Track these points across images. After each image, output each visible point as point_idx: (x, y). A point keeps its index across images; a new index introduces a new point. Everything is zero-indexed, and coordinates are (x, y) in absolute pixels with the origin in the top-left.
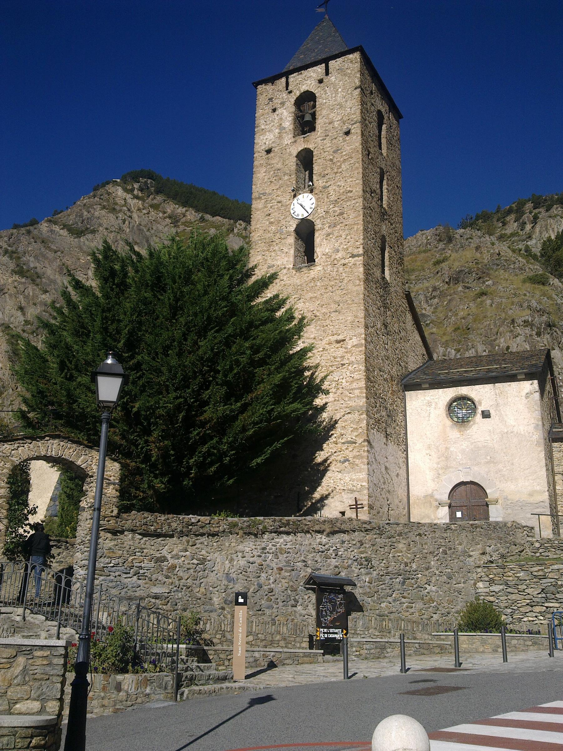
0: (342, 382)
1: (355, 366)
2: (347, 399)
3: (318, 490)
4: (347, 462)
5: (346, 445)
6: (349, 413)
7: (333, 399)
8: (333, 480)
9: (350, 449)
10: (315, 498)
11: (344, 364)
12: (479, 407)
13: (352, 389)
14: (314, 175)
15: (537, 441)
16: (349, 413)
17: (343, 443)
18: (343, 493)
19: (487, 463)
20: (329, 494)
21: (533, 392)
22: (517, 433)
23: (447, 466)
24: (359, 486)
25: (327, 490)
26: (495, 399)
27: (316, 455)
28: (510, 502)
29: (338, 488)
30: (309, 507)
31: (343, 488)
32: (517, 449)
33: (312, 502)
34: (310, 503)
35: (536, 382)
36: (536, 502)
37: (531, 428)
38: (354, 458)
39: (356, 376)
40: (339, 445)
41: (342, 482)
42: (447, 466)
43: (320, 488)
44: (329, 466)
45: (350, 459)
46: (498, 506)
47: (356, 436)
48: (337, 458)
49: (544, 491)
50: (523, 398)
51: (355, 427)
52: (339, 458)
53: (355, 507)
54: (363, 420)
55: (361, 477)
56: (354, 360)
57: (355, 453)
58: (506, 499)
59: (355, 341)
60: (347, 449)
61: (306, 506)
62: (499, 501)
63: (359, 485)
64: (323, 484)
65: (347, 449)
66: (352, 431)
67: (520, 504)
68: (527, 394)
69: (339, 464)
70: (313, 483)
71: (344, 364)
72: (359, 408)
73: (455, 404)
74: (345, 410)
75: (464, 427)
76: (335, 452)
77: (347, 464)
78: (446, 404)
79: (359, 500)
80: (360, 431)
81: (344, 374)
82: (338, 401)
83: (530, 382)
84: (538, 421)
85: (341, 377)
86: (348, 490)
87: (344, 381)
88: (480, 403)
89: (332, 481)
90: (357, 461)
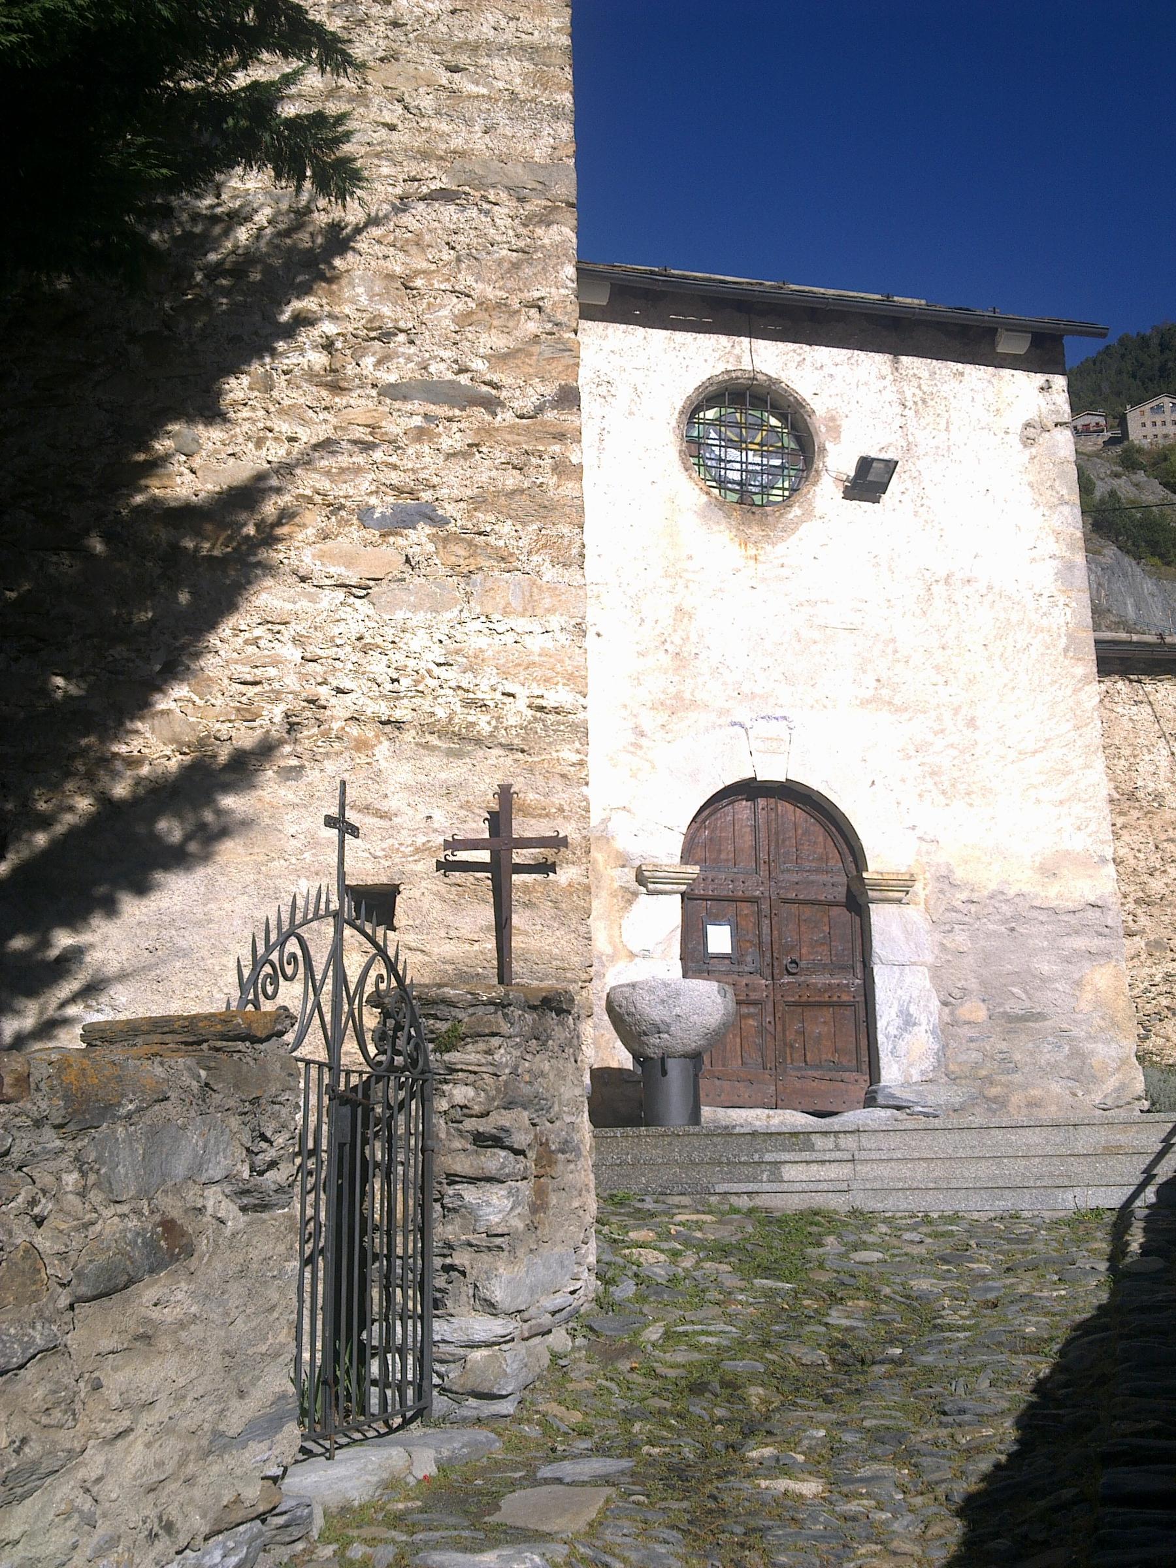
2: (427, 103)
3: (163, 703)
4: (423, 531)
5: (415, 406)
6: (444, 196)
8: (297, 641)
9: (451, 440)
10: (133, 762)
12: (829, 446)
15: (1069, 636)
18: (383, 749)
19: (864, 703)
20: (266, 750)
21: (1050, 425)
22: (990, 588)
23: (678, 696)
24: (517, 712)
25: (248, 714)
26: (899, 421)
27: (162, 445)
28: (964, 896)
29: (339, 708)
30: (73, 833)
32: (989, 659)
33: (105, 800)
34: (84, 804)
35: (1060, 382)
36: (1071, 906)
37: (1045, 576)
38: (478, 502)
42: (678, 696)
43: (180, 691)
44: (268, 537)
45: (449, 509)
46: (914, 913)
47: (499, 358)
48: (338, 491)
49: (1103, 860)
50: (1015, 440)
51: (492, 293)
52: (359, 489)
53: (484, 856)
54: (554, 255)
55: (535, 644)
58: (946, 880)
61: (45, 822)
62: (918, 886)
63: (521, 703)
64: (210, 664)
66: (464, 320)
67: (1005, 908)
68: (1028, 425)
69: (356, 533)
70: (119, 651)
73: (711, 414)
75: (762, 523)
77: (419, 537)
78: (679, 405)
79: (527, 812)
80: (532, 327)
83: (1039, 379)
84: (1071, 546)
86: (430, 727)
88: (835, 430)
89: (294, 654)
90: (506, 528)
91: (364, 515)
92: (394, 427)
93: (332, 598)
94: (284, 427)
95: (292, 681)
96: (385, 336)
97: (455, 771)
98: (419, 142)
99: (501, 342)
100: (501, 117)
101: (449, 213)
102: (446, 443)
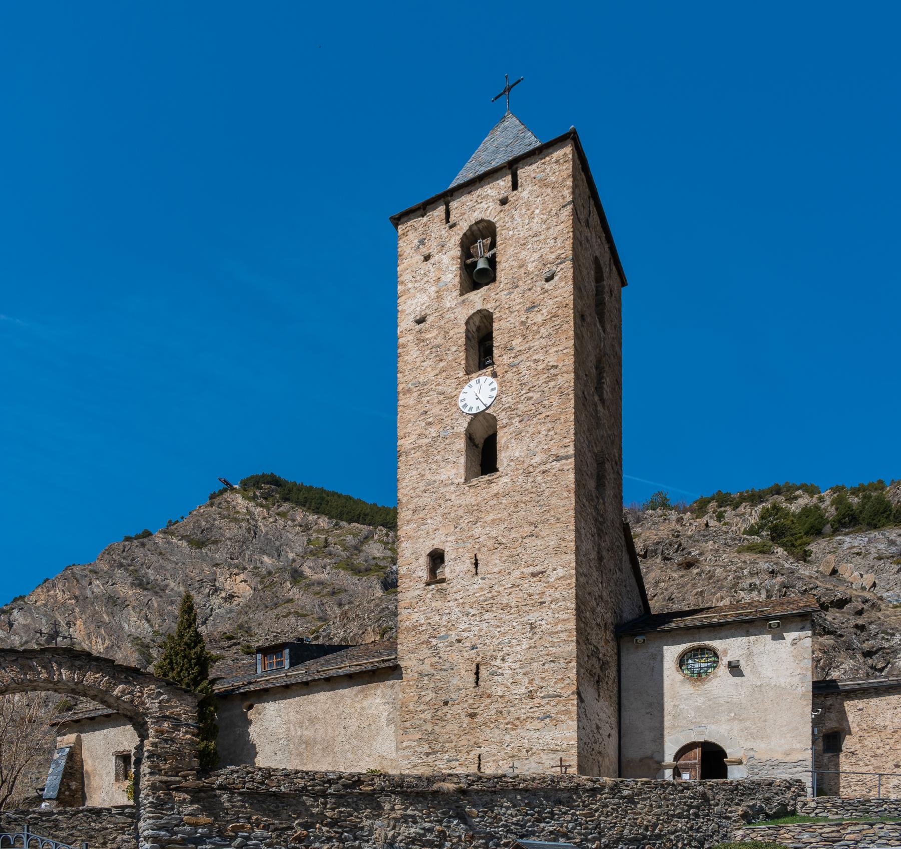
0: (541, 625)
1: (560, 604)
4: (548, 719)
6: (551, 661)
7: (528, 646)
8: (528, 739)
9: (553, 703)
11: (544, 602)
13: (557, 633)
14: (494, 349)
16: (551, 661)
17: (543, 697)
31: (542, 748)
39: (562, 616)
40: (537, 701)
41: (541, 741)
51: (560, 677)
52: (537, 715)
54: (571, 669)
56: (558, 596)
57: (559, 708)
59: (561, 572)
60: (547, 704)
65: (547, 704)
71: (544, 602)
72: (565, 654)
74: (545, 658)
76: (531, 708)
80: (568, 682)
81: (544, 615)
82: (535, 647)
85: (540, 618)
87: (543, 623)
90: (563, 717)
91: (538, 718)
92: (542, 703)
93: (532, 732)
94: (524, 706)
95: (527, 745)
96: (541, 688)
97: (554, 756)
98: (546, 653)
99: (562, 685)
100: (562, 645)
101: (552, 664)
102: (552, 704)
